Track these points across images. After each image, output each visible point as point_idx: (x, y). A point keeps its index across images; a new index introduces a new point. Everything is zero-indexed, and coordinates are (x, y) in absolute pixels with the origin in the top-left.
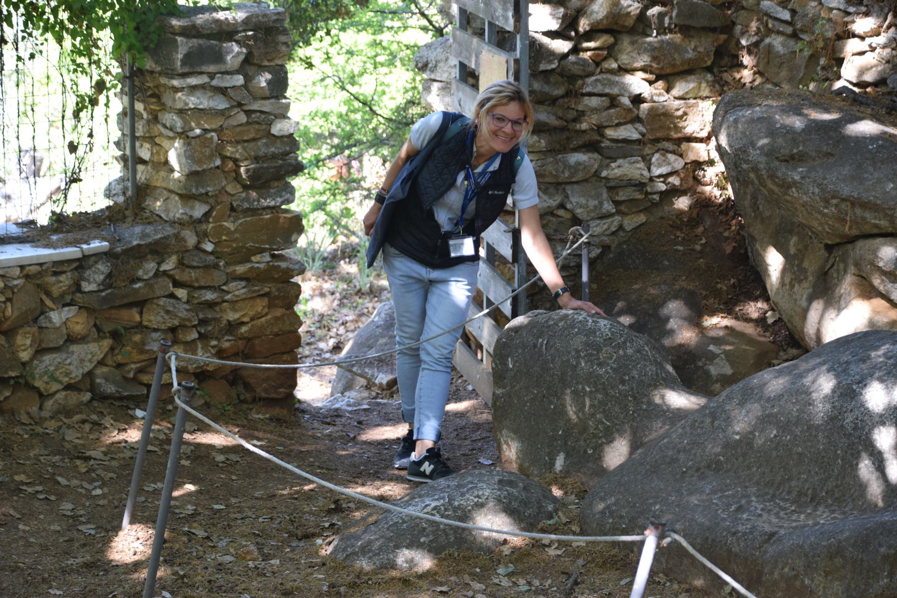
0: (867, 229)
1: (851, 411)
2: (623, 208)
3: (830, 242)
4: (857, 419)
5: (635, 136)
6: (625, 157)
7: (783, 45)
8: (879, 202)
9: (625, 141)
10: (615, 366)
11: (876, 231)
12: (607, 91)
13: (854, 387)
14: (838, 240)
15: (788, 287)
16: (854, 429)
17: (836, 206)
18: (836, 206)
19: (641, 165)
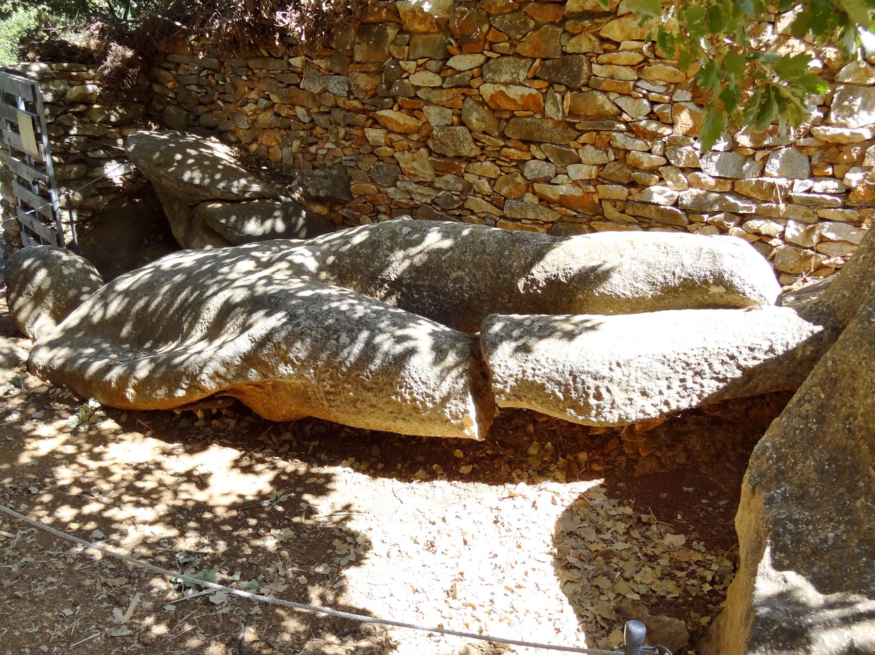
2: (103, 191)
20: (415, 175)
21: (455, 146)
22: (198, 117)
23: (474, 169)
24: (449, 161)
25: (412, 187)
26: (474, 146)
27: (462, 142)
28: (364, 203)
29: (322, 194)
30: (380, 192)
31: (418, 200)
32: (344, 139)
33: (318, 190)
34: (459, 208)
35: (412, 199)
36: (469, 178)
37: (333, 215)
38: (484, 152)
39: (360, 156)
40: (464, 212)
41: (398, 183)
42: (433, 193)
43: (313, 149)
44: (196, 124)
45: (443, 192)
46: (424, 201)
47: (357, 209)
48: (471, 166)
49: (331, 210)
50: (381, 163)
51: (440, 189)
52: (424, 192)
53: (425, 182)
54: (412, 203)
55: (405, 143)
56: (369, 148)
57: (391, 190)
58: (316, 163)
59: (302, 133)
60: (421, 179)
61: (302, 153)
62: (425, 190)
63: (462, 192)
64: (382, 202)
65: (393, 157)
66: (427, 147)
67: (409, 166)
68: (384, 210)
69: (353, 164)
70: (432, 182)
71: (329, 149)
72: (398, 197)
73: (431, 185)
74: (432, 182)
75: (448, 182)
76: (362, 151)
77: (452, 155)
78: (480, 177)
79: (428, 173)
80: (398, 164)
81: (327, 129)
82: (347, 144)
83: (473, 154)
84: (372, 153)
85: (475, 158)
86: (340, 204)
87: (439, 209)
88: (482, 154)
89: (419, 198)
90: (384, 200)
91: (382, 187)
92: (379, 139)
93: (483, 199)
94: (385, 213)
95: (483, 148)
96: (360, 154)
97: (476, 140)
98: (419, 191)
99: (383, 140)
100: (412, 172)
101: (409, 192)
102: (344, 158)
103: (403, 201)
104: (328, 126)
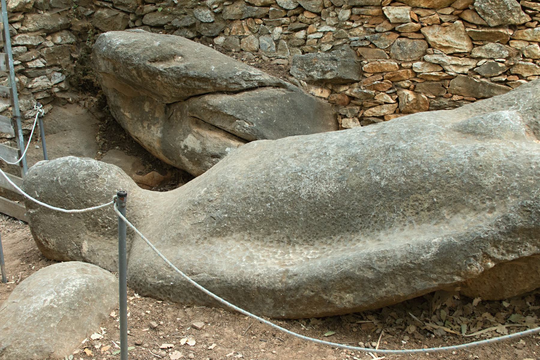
0: (200, 92)
1: (303, 188)
3: (169, 102)
4: (309, 192)
5: (42, 65)
6: (38, 76)
7: (108, 13)
8: (209, 77)
9: (38, 68)
10: (108, 185)
11: (204, 92)
12: (25, 43)
13: (300, 174)
14: (174, 101)
15: (147, 128)
16: (309, 198)
17: (185, 82)
18: (185, 82)
19: (47, 80)
20: (448, 47)
21: (501, 15)
22: (142, 17)
23: (523, 35)
24: (493, 30)
25: (446, 59)
26: (524, 14)
27: (510, 11)
28: (382, 80)
29: (328, 76)
30: (400, 67)
31: (452, 71)
32: (349, 20)
33: (324, 73)
34: (504, 73)
35: (444, 71)
36: (517, 44)
37: (335, 97)
38: (535, 18)
39: (376, 35)
40: (511, 78)
41: (427, 57)
42: (472, 64)
43: (301, 34)
44: (137, 24)
45: (484, 61)
46: (460, 70)
47: (373, 87)
48: (520, 33)
49: (332, 92)
50: (404, 40)
51: (480, 58)
52: (460, 63)
53: (460, 53)
54: (444, 75)
55: (437, 17)
56: (390, 27)
57: (418, 65)
58: (307, 48)
59: (285, 20)
60: (457, 51)
61: (288, 40)
62: (460, 61)
63: (507, 58)
64: (405, 77)
65: (419, 32)
66: (460, 19)
67: (440, 39)
68: (407, 85)
69: (367, 43)
70: (470, 53)
71: (324, 33)
72: (426, 71)
73: (468, 55)
74: (470, 53)
75: (490, 50)
76: (377, 29)
77: (495, 24)
78: (530, 42)
79: (464, 46)
80: (425, 39)
81: (319, 14)
82: (355, 25)
83: (522, 22)
84: (393, 30)
85: (524, 25)
86: (345, 84)
87: (479, 77)
88: (532, 21)
89: (454, 68)
90: (407, 74)
91: (405, 62)
92: (404, 16)
93: (534, 63)
94: (408, 88)
95: (531, 15)
96: (376, 32)
97: (524, 8)
98: (454, 62)
99: (409, 17)
100: (444, 45)
101: (439, 65)
102: (353, 38)
103: (434, 74)
104: (320, 10)
